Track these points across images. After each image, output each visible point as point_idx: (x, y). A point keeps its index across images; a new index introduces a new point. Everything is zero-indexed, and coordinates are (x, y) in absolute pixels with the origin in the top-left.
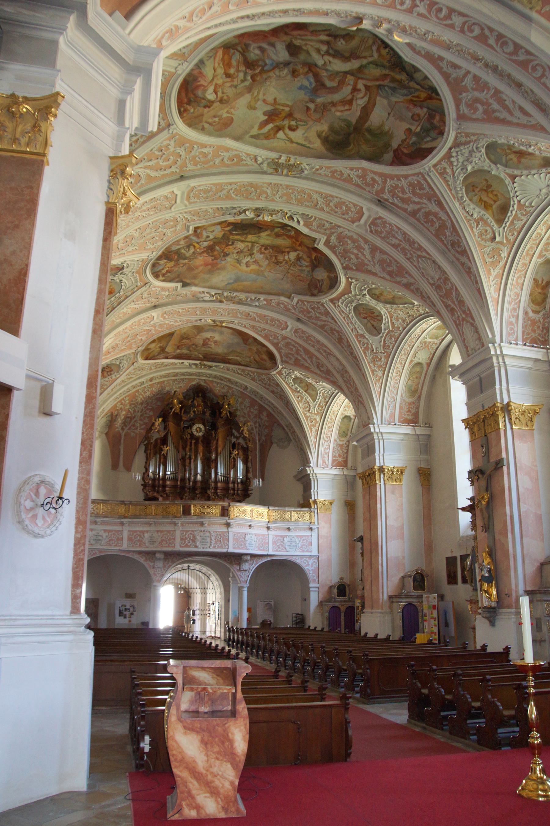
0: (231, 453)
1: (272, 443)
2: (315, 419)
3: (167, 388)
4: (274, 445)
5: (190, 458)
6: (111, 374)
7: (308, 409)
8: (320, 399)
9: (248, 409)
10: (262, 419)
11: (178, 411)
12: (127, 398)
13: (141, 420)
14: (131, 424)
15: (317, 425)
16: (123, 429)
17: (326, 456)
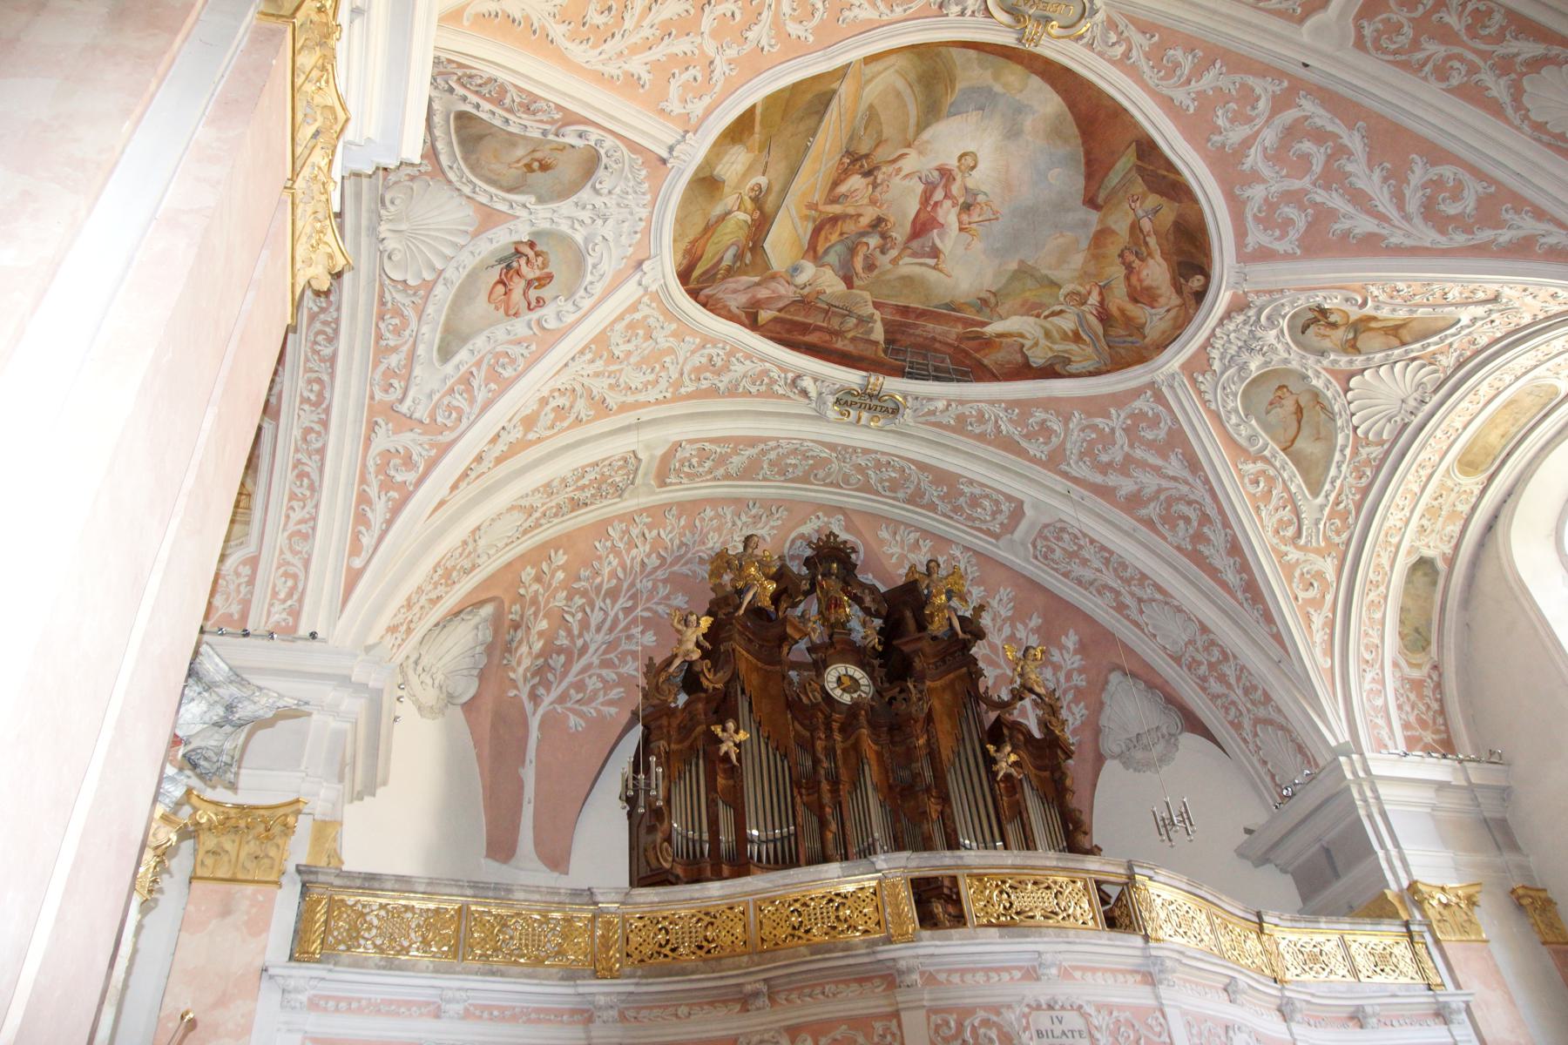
0: (990, 761)
1: (1100, 760)
2: (1320, 575)
3: (714, 543)
4: (1111, 768)
5: (835, 783)
6: (540, 302)
7: (1291, 532)
8: (1340, 475)
9: (1007, 631)
10: (1056, 668)
11: (766, 602)
12: (561, 558)
13: (606, 664)
14: (570, 678)
15: (1329, 598)
16: (534, 697)
17: (1381, 721)
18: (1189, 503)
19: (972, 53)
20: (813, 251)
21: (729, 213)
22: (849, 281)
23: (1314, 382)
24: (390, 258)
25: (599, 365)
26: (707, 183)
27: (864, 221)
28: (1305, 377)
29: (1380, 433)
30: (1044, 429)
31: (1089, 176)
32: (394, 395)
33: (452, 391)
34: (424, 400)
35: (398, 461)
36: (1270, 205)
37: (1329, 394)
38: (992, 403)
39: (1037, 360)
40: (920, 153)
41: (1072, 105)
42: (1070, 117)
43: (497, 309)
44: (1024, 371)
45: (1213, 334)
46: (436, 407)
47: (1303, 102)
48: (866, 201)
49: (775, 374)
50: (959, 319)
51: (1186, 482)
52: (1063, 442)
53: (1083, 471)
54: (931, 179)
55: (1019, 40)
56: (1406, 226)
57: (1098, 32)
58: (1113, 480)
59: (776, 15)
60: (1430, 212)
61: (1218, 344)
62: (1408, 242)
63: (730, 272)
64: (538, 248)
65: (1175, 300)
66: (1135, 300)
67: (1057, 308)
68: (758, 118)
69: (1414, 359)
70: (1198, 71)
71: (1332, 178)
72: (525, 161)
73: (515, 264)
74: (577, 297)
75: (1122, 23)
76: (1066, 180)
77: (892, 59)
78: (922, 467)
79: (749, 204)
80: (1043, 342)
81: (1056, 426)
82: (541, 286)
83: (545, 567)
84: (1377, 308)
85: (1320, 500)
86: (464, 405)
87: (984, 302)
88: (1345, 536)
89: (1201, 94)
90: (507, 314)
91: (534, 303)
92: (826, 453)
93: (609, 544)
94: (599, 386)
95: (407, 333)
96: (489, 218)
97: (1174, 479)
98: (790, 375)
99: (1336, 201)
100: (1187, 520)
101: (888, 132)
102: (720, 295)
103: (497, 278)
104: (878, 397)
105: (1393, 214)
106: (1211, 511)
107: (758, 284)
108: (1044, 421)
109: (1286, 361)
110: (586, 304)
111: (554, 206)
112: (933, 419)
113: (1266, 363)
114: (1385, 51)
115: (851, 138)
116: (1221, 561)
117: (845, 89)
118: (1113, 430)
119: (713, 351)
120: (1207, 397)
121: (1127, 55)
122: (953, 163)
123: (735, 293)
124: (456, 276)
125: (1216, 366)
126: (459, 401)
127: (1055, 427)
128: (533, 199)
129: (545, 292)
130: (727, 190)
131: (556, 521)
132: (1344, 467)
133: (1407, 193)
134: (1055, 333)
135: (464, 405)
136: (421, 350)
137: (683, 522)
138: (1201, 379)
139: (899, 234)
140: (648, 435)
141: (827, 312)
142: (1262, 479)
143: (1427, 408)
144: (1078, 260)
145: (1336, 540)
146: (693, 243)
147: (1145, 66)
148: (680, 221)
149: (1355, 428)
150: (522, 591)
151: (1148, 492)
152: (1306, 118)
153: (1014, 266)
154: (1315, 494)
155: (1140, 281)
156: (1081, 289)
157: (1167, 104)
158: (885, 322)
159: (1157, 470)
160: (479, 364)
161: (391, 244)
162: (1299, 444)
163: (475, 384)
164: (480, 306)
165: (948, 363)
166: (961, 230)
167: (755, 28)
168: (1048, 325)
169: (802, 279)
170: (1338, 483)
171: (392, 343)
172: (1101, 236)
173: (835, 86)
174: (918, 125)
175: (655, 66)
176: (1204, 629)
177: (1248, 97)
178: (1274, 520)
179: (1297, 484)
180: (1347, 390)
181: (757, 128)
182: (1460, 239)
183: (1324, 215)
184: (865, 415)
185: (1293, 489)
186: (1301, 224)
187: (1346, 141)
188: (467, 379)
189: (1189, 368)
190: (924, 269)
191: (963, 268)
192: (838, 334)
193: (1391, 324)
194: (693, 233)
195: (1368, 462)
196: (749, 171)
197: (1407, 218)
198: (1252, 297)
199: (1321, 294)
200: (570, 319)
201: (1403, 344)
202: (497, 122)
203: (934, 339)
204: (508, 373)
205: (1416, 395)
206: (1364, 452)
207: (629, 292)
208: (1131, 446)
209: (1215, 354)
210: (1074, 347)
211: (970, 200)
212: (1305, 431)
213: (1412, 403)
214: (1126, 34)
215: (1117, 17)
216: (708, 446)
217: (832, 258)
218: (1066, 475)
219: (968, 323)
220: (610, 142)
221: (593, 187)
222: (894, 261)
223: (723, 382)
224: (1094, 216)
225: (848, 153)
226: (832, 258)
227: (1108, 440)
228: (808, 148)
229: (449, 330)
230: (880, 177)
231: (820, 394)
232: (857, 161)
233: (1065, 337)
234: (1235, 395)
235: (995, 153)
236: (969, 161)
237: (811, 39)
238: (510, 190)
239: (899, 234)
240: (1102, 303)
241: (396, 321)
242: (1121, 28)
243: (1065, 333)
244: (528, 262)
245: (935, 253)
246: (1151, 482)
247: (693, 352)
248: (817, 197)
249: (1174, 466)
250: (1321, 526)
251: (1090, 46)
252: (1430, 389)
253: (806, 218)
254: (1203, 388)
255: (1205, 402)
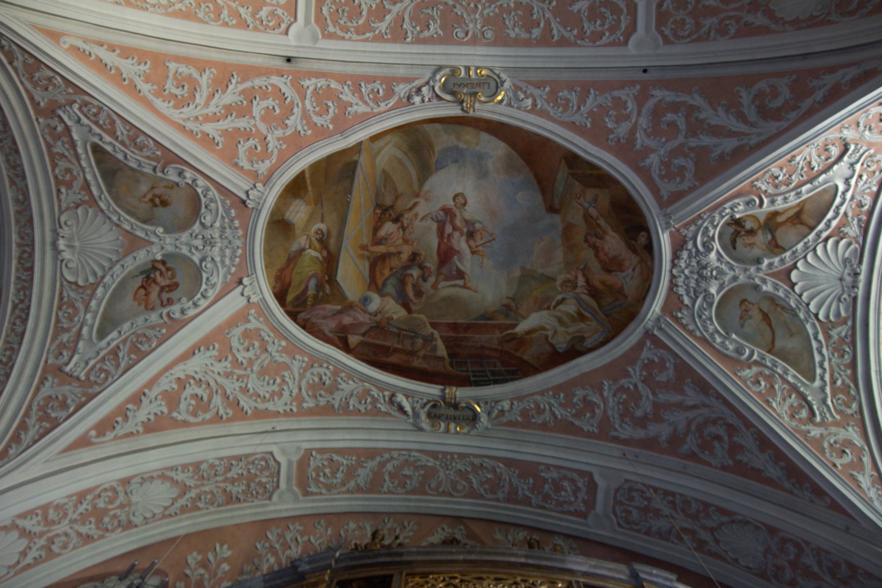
2: (849, 443)
6: (170, 302)
7: (804, 413)
8: (824, 358)
15: (866, 459)
18: (714, 422)
19: (438, 126)
20: (374, 284)
21: (303, 250)
22: (406, 306)
23: (764, 288)
24: (66, 265)
25: (227, 364)
26: (280, 225)
27: (405, 257)
28: (756, 287)
29: (838, 314)
30: (589, 405)
31: (543, 191)
32: (61, 361)
33: (103, 359)
34: (83, 365)
35: (56, 404)
36: (666, 164)
37: (781, 293)
38: (542, 393)
39: (562, 347)
40: (427, 200)
41: (513, 145)
42: (515, 154)
43: (139, 305)
44: (557, 358)
45: (673, 277)
46: (92, 369)
47: (654, 93)
48: (400, 242)
49: (375, 392)
50: (494, 326)
51: (705, 405)
52: (605, 411)
53: (626, 431)
54: (440, 218)
55: (462, 109)
56: (756, 130)
57: (511, 95)
58: (653, 429)
59: (304, 110)
60: (765, 113)
61: (680, 281)
62: (762, 138)
63: (318, 300)
64: (168, 265)
65: (635, 259)
66: (609, 271)
67: (559, 297)
68: (308, 181)
69: (826, 240)
70: (582, 101)
71: (695, 127)
72: (149, 197)
73: (152, 275)
74: (196, 298)
75: (523, 86)
76: (528, 199)
77: (388, 138)
78: (509, 463)
79: (317, 244)
80: (561, 329)
81: (595, 399)
82: (170, 291)
83: (211, 556)
84: (773, 202)
85: (817, 383)
86: (112, 369)
87: (507, 306)
88: (854, 406)
89: (591, 113)
90: (146, 308)
91: (165, 302)
92: (431, 462)
93: (267, 545)
94: (232, 387)
95: (76, 319)
96: (133, 243)
97: (695, 407)
98: (387, 393)
99: (706, 140)
100: (718, 438)
101: (401, 188)
102: (314, 320)
103: (139, 284)
104: (456, 406)
105: (743, 128)
106: (733, 420)
107: (340, 312)
108: (585, 397)
109: (735, 278)
110: (203, 304)
111: (177, 236)
112: (504, 420)
113: (721, 287)
114: (683, 37)
115: (377, 195)
116: (759, 460)
117: (363, 160)
118: (635, 386)
119: (321, 370)
120: (691, 327)
121: (534, 104)
122: (450, 203)
123: (326, 314)
124: (112, 281)
125: (686, 301)
126: (108, 366)
127: (595, 400)
128: (160, 230)
129: (174, 295)
130: (298, 232)
131: (212, 509)
132: (824, 351)
133: (745, 111)
134: (565, 318)
135: (112, 369)
136: (85, 331)
137: (329, 532)
138: (680, 315)
139: (431, 264)
140: (281, 438)
141: (399, 335)
142: (761, 379)
143: (862, 277)
144: (559, 255)
145: (849, 411)
146: (282, 270)
147: (549, 108)
148: (268, 252)
149: (816, 315)
150: (188, 572)
151: (681, 426)
152: (660, 101)
153: (517, 273)
154: (812, 380)
155: (606, 254)
156: (569, 276)
157: (572, 126)
158: (445, 340)
159: (680, 406)
160: (124, 342)
161: (67, 255)
162: (779, 344)
163: (121, 355)
164: (128, 302)
165: (499, 367)
166: (473, 253)
167: (292, 118)
168: (558, 314)
169: (373, 307)
170: (826, 365)
171: (66, 326)
172: (568, 231)
173: (355, 158)
174: (419, 180)
175: (225, 133)
176: (772, 531)
177: (620, 104)
178: (786, 408)
179: (792, 376)
180: (792, 285)
181: (310, 188)
182: (793, 115)
183: (702, 152)
184: (452, 426)
185: (790, 379)
186: (690, 165)
187: (692, 102)
188: (115, 352)
189: (667, 308)
190: (457, 289)
191: (485, 284)
192: (412, 353)
193: (791, 213)
194: (281, 262)
195: (842, 340)
196: (311, 219)
197: (752, 125)
198: (684, 232)
199: (727, 205)
200: (191, 313)
201: (812, 229)
202: (120, 156)
203: (482, 347)
204: (145, 348)
205: (847, 271)
206: (834, 333)
207: (234, 302)
208: (654, 394)
209: (681, 291)
210: (582, 325)
211: (471, 229)
212: (779, 333)
213: (849, 279)
214: (529, 92)
215: (519, 84)
216: (336, 457)
217: (390, 289)
218: (616, 440)
219: (502, 328)
220: (201, 182)
221: (202, 224)
222: (434, 286)
223: (337, 399)
224: (557, 218)
225: (378, 206)
226: (390, 289)
227: (635, 396)
228: (348, 203)
229: (104, 318)
230: (405, 222)
231: (413, 409)
232: (385, 212)
233: (573, 320)
234: (710, 319)
235: (473, 189)
236: (460, 200)
237: (331, 127)
238: (145, 222)
239: (431, 264)
240: (587, 281)
241: (70, 311)
242: (524, 89)
243: (572, 316)
244: (161, 274)
245: (461, 275)
246: (679, 418)
247: (305, 370)
248: (366, 240)
249: (692, 396)
250: (829, 402)
251: (509, 105)
252: (855, 262)
253: (362, 257)
254: (684, 321)
255: (691, 333)
